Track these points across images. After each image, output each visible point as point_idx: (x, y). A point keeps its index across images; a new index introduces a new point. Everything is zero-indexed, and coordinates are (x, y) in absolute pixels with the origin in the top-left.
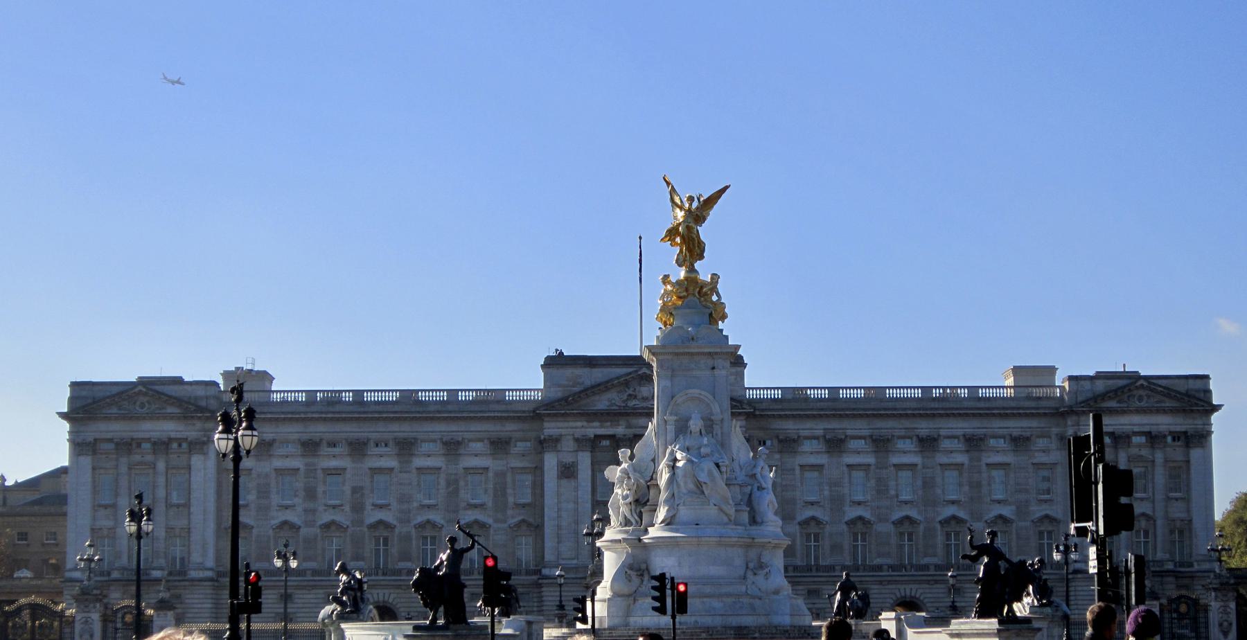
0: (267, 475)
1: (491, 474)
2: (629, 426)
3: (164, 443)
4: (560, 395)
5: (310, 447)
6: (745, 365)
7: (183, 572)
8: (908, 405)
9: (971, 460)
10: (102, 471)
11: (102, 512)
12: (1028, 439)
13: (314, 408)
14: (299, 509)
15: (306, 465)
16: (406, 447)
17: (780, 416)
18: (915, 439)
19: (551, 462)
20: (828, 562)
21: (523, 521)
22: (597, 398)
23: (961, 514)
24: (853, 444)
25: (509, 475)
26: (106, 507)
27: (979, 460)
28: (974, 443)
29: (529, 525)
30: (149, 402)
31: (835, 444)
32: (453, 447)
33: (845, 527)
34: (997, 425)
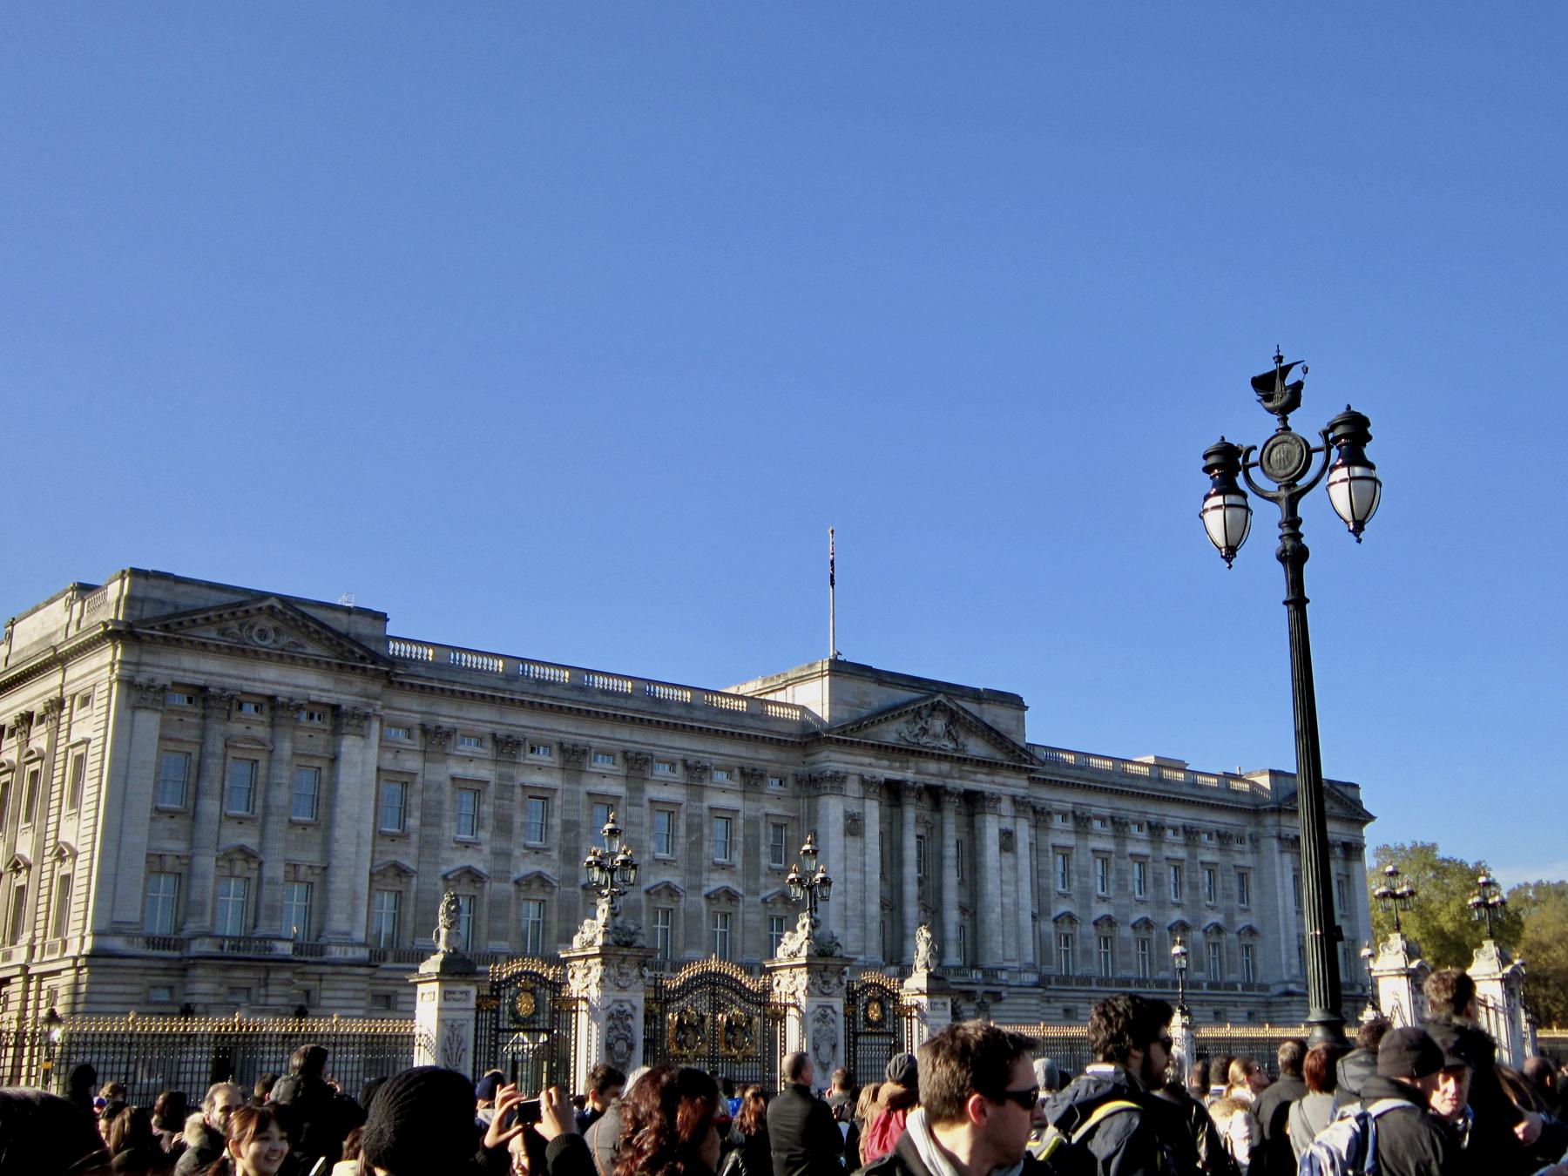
1: (741, 822)
2: (918, 772)
3: (299, 708)
5: (507, 747)
7: (321, 950)
10: (171, 746)
11: (164, 823)
13: (516, 686)
14: (486, 849)
15: (500, 776)
16: (637, 765)
19: (833, 809)
20: (1078, 973)
22: (884, 726)
24: (1097, 824)
25: (762, 825)
26: (172, 814)
28: (1190, 834)
30: (276, 630)
31: (1081, 822)
32: (696, 773)
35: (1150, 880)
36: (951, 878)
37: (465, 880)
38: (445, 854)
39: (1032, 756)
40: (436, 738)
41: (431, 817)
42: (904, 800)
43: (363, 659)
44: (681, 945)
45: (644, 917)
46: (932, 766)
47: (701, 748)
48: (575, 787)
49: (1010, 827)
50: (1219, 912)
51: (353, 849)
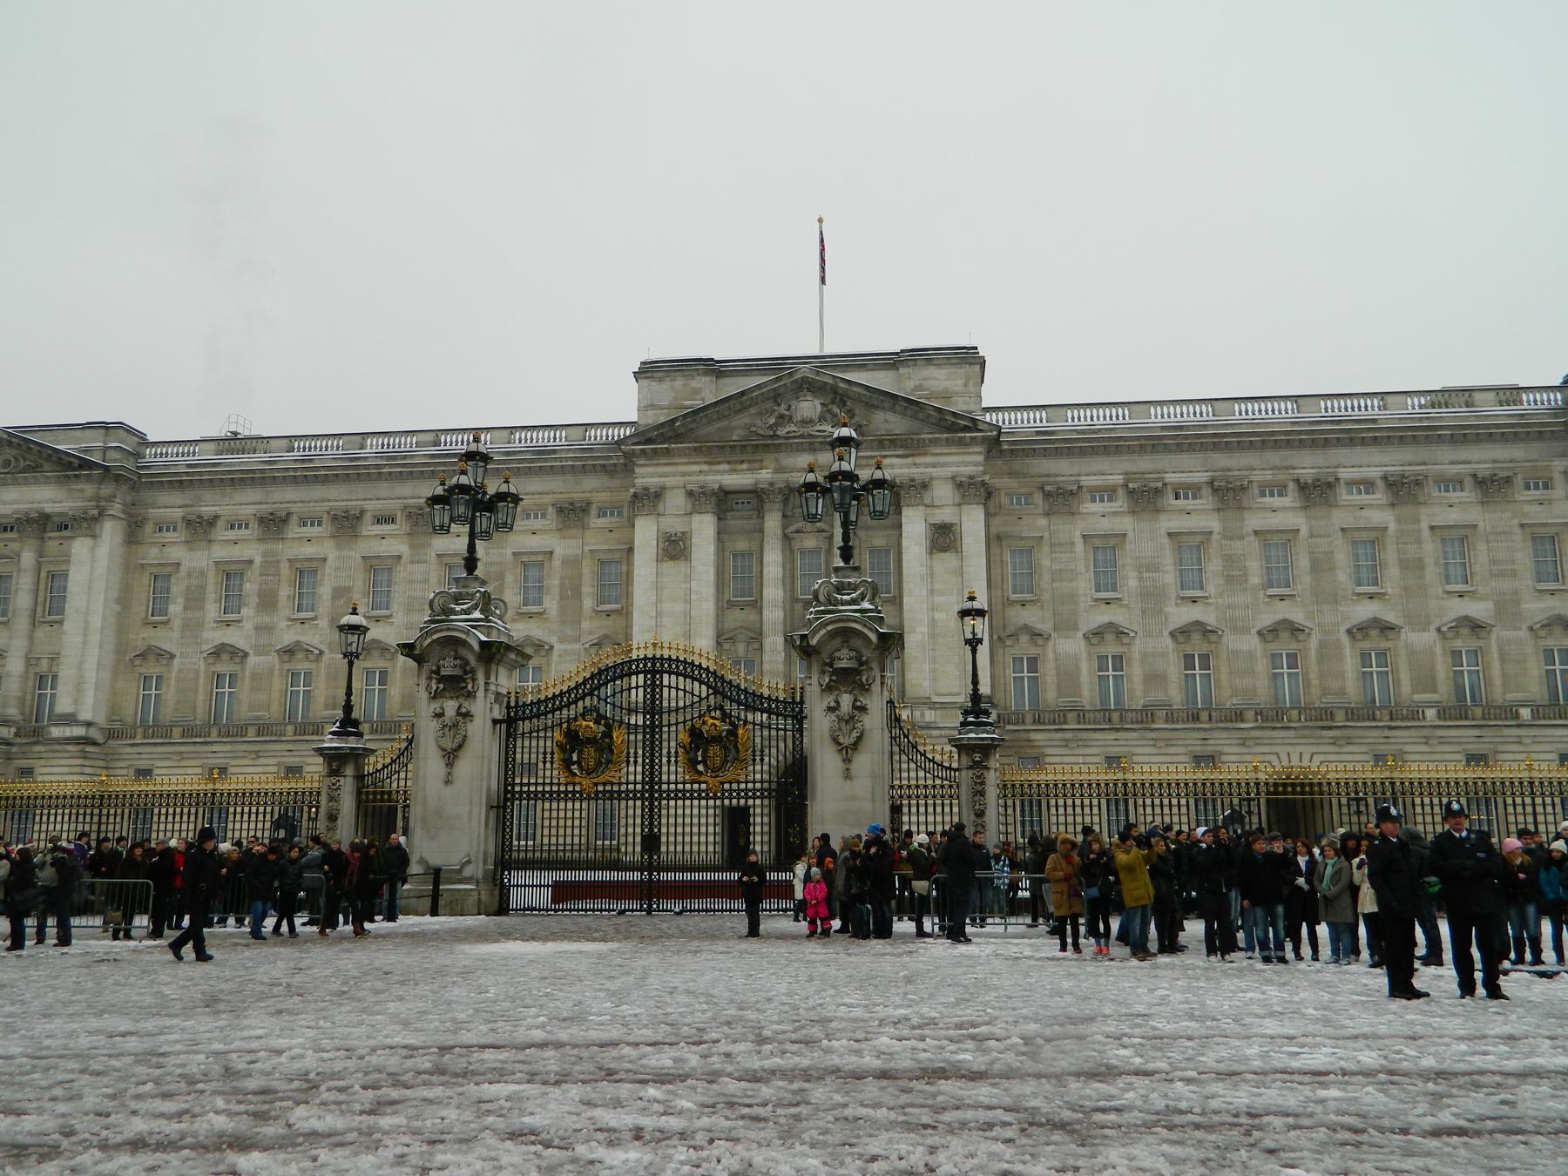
0: (202, 573)
2: (779, 469)
4: (662, 419)
5: (274, 524)
9: (1399, 520)
12: (1508, 480)
14: (248, 626)
15: (264, 554)
17: (1046, 453)
18: (1291, 486)
19: (646, 533)
21: (606, 636)
23: (1391, 617)
27: (1418, 521)
28: (1402, 489)
31: (1145, 497)
33: (1168, 642)
34: (1446, 460)
35: (1303, 563)
37: (225, 657)
38: (205, 635)
39: (974, 421)
40: (200, 528)
41: (195, 600)
43: (81, 467)
46: (804, 460)
48: (346, 553)
49: (948, 519)
50: (1481, 599)
51: (80, 639)
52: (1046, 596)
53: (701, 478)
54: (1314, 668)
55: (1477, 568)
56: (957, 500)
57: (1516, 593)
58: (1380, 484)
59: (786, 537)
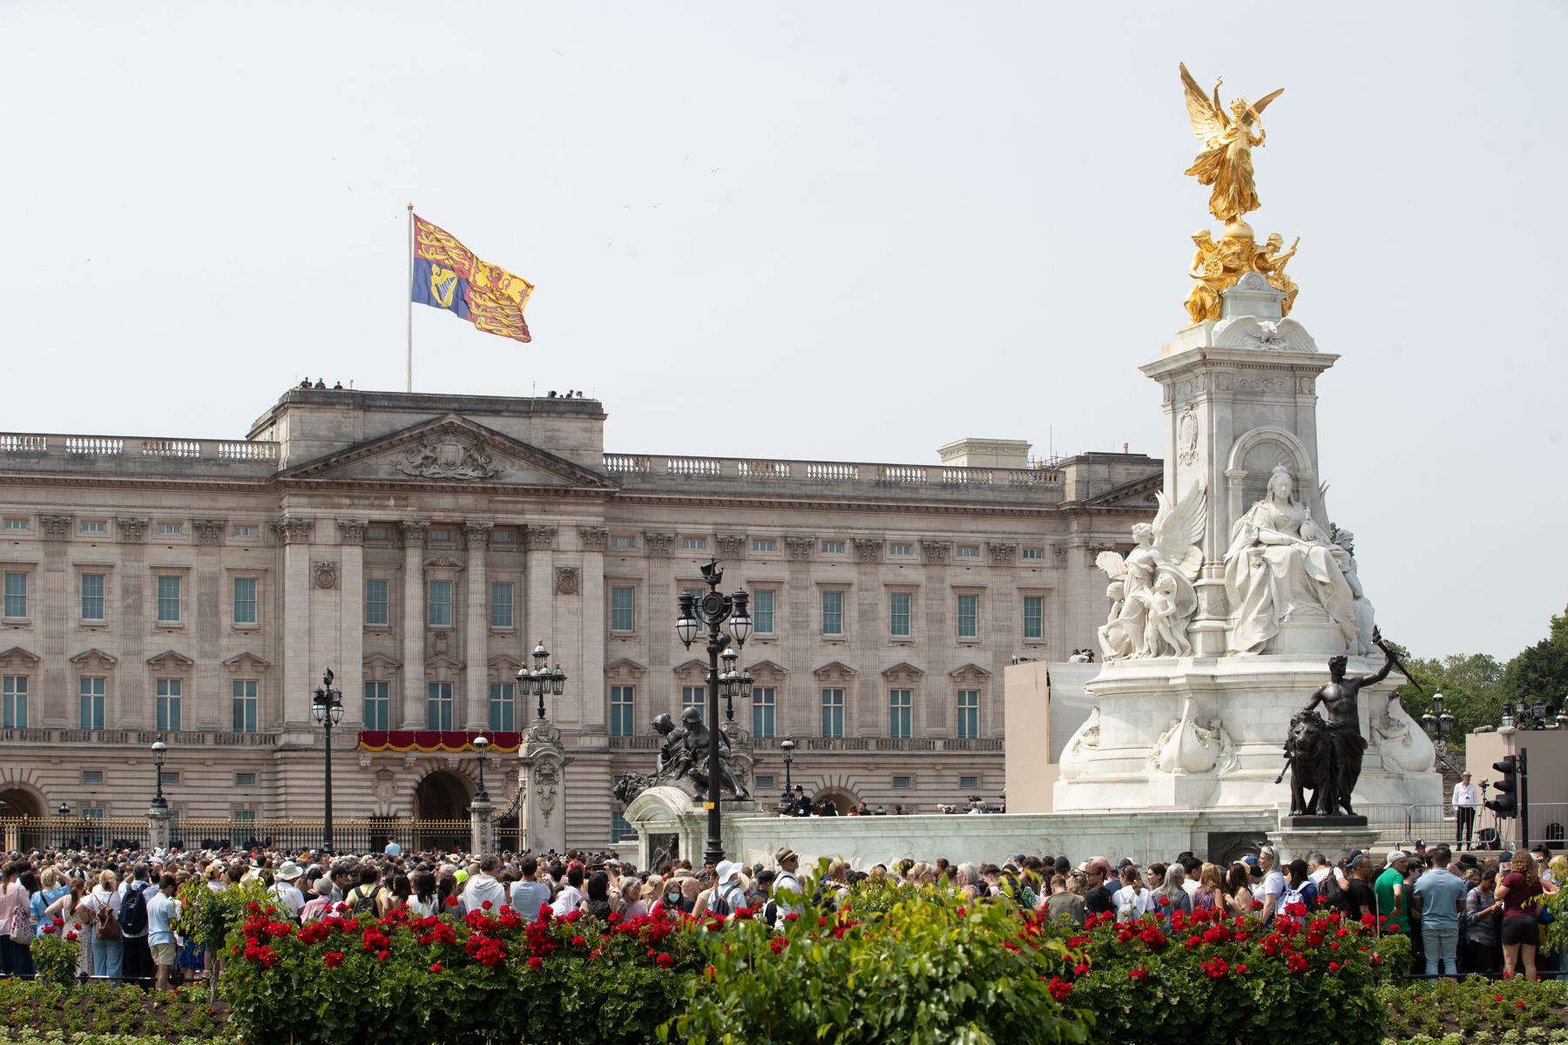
6: (603, 417)
8: (839, 491)
9: (929, 579)
12: (1012, 550)
18: (848, 544)
19: (297, 561)
21: (247, 656)
22: (372, 461)
23: (916, 662)
27: (942, 580)
28: (934, 552)
29: (256, 662)
32: (133, 531)
36: (476, 628)
39: (601, 477)
42: (408, 543)
44: (117, 714)
45: (69, 687)
46: (447, 501)
47: (140, 503)
50: (984, 649)
52: (644, 633)
53: (351, 511)
54: (855, 704)
55: (982, 623)
56: (580, 546)
57: (1010, 646)
58: (917, 546)
59: (425, 572)
